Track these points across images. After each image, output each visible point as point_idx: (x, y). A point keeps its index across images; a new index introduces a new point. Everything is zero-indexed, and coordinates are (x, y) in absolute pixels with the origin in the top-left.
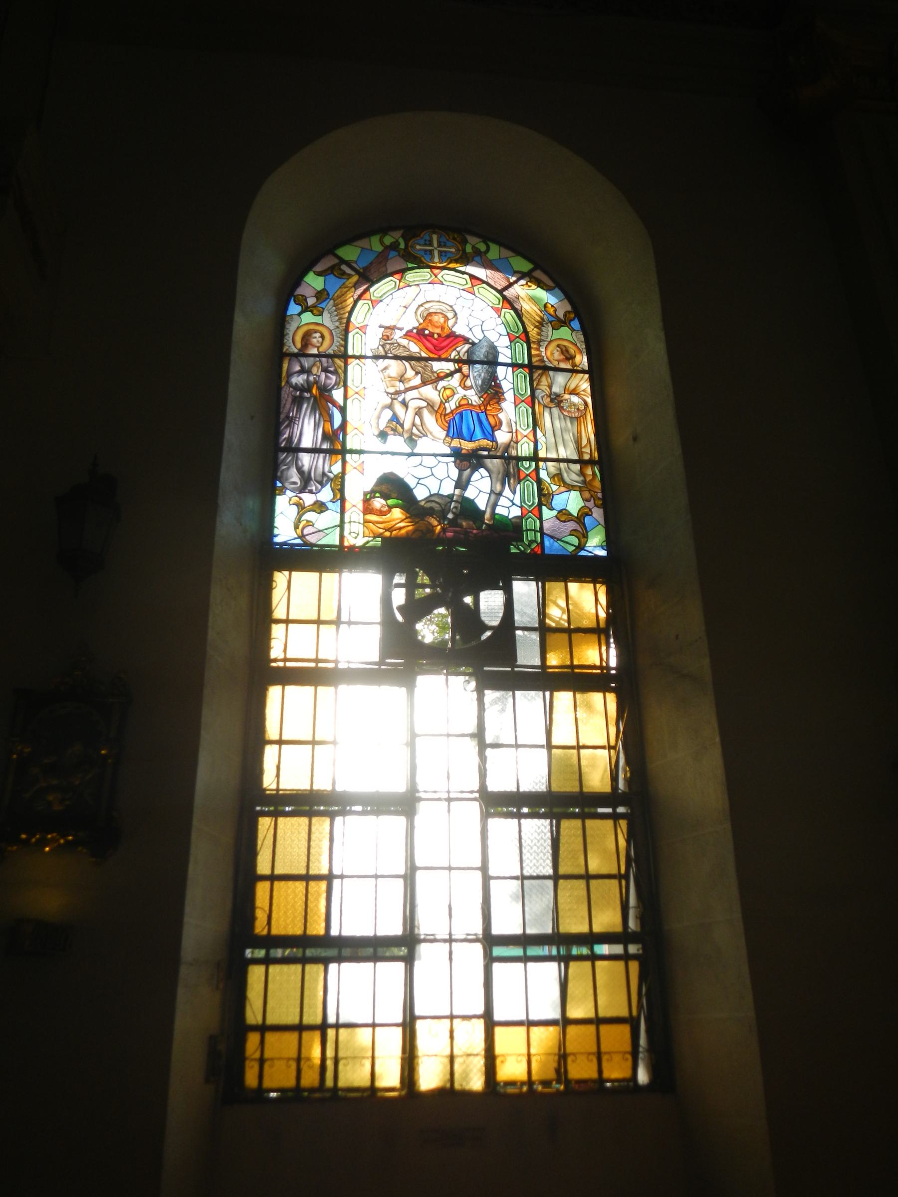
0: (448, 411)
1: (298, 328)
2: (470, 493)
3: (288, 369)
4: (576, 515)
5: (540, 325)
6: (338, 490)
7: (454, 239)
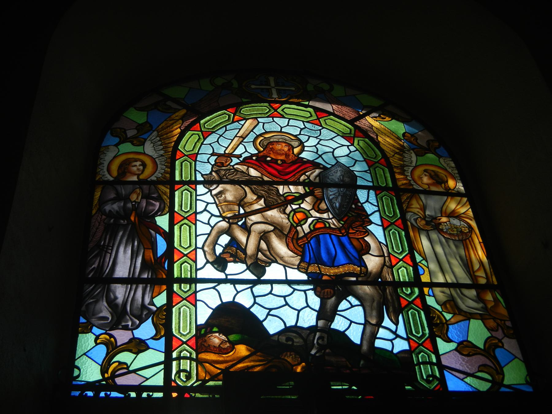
0: (301, 234)
1: (115, 157)
2: (339, 324)
3: (100, 197)
4: (482, 347)
5: (402, 150)
6: (161, 324)
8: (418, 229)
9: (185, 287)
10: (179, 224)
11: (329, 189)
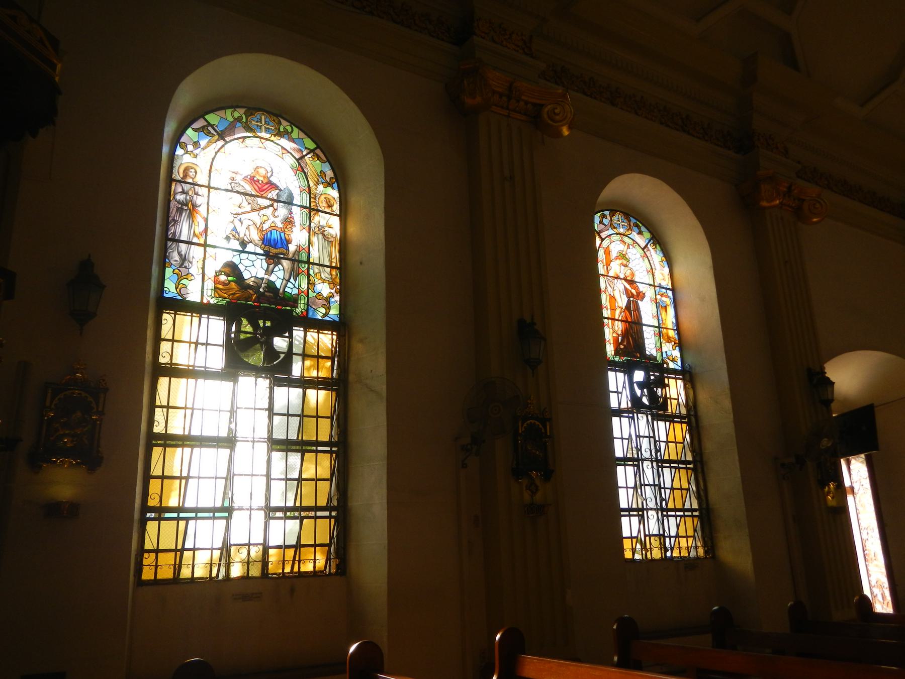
2: (273, 278)
7: (274, 121)
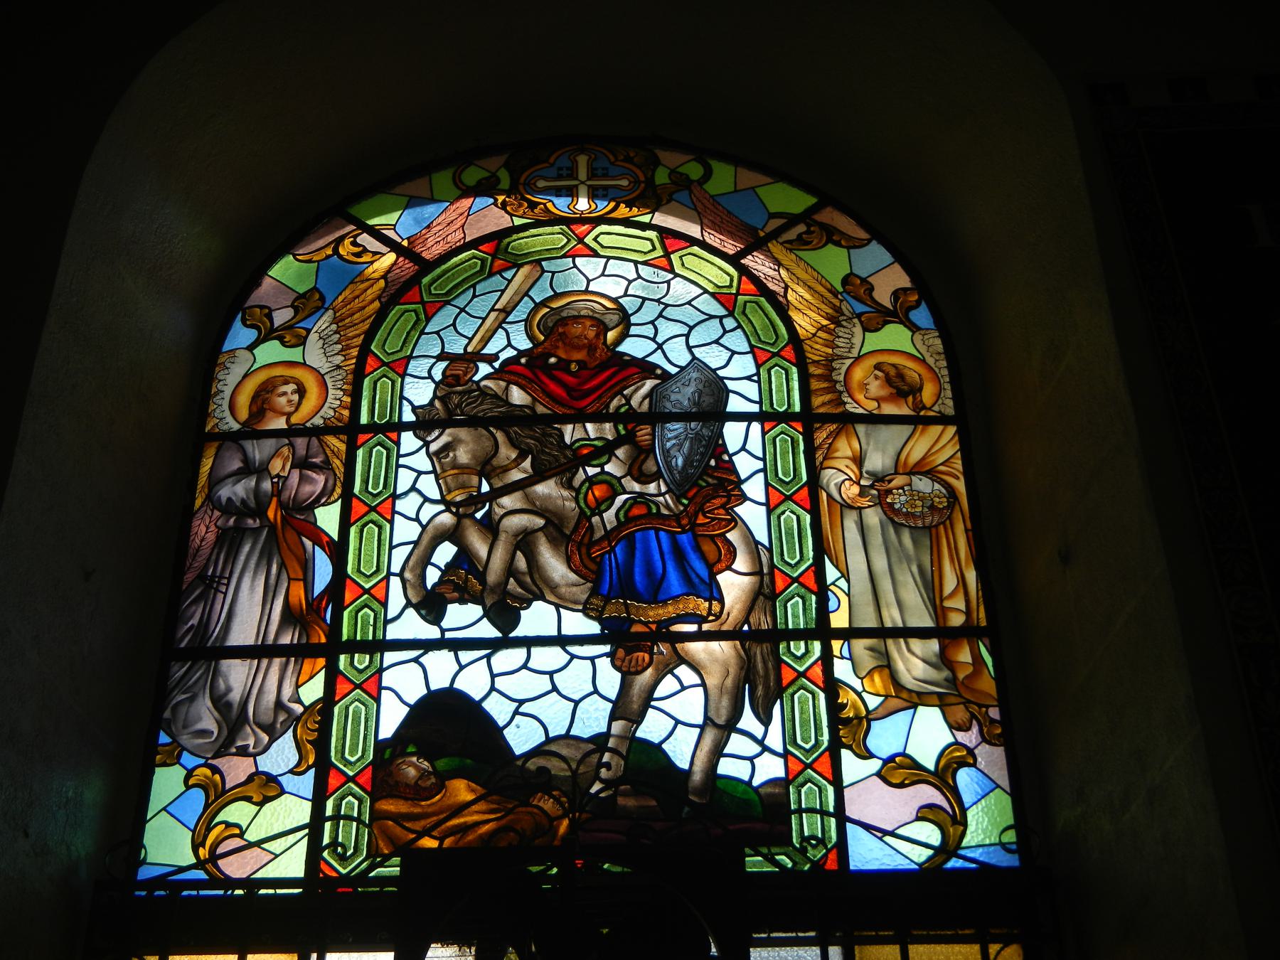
0: (599, 533)
1: (246, 376)
2: (652, 728)
3: (212, 468)
4: (931, 767)
7: (628, 159)
8: (842, 505)
9: (362, 660)
10: (359, 524)
11: (668, 425)
